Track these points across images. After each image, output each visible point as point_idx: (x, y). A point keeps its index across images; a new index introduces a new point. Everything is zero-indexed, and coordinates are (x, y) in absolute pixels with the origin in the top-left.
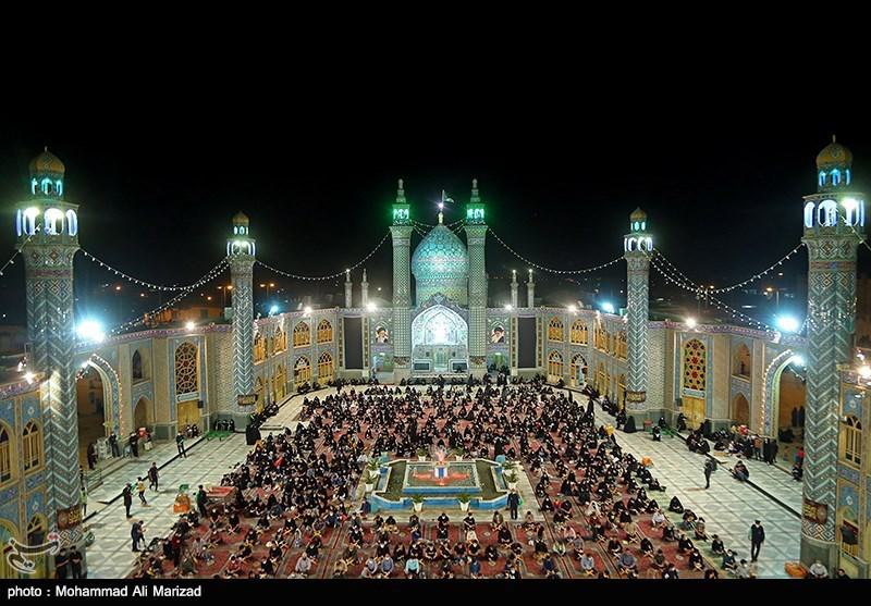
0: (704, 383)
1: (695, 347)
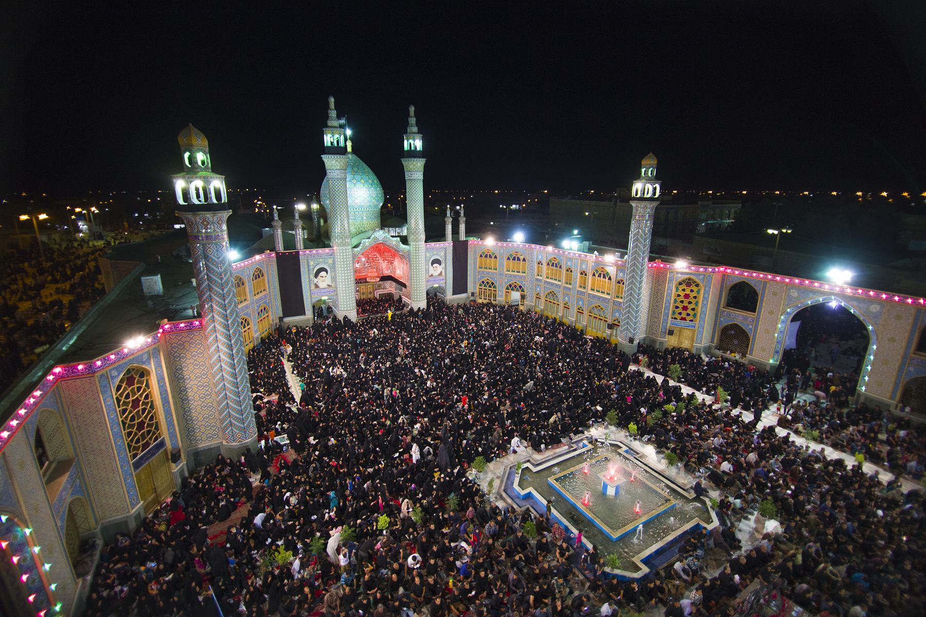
0: (695, 315)
1: (688, 285)
